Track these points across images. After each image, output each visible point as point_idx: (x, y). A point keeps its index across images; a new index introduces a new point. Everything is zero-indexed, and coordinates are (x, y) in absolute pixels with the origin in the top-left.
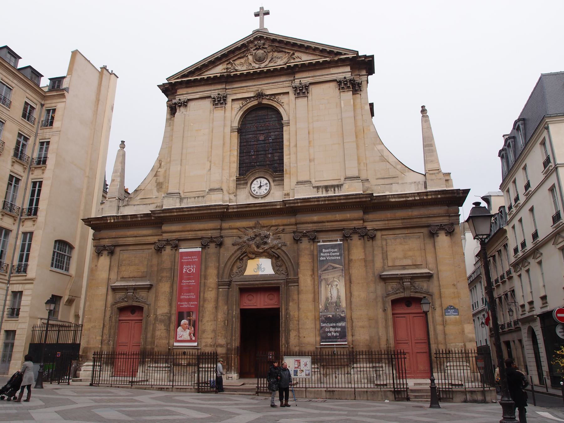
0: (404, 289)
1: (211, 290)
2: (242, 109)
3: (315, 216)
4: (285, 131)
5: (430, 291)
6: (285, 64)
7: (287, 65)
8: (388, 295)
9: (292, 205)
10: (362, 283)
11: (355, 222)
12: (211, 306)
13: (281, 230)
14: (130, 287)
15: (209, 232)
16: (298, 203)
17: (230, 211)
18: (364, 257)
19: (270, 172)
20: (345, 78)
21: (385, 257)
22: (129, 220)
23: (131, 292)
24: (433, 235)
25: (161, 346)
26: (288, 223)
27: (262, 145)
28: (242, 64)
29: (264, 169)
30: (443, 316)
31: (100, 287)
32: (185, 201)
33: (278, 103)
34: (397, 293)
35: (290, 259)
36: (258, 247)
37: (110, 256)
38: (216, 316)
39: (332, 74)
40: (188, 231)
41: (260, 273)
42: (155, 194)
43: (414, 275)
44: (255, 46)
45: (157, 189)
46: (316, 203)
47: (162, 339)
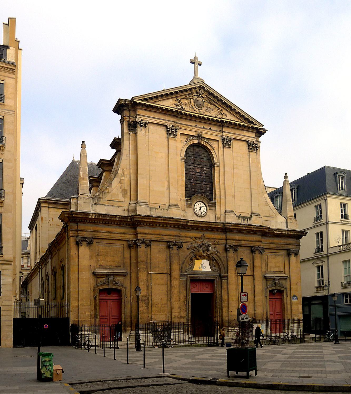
0: (275, 285)
1: (176, 280)
2: (187, 144)
3: (237, 236)
4: (216, 170)
5: (286, 287)
6: (220, 119)
7: (221, 119)
8: (268, 288)
9: (228, 227)
10: (260, 280)
11: (257, 243)
12: (177, 291)
13: (217, 242)
14: (111, 274)
15: (173, 237)
16: (231, 226)
17: (189, 224)
18: (261, 265)
19: (207, 199)
20: (253, 142)
21: (267, 266)
22: (109, 219)
23: (112, 278)
24: (289, 255)
25: (144, 319)
26: (221, 238)
27: (199, 176)
28: (186, 104)
29: (203, 196)
30: (291, 300)
31: (83, 272)
32: (154, 210)
33: (211, 146)
34: (272, 287)
35: (222, 262)
36: (203, 252)
37: (89, 246)
38: (180, 298)
39: (245, 136)
40: (158, 235)
41: (203, 270)
42: (121, 198)
43: (281, 277)
44: (197, 93)
45: (122, 195)
46: (241, 228)
47: (144, 314)
